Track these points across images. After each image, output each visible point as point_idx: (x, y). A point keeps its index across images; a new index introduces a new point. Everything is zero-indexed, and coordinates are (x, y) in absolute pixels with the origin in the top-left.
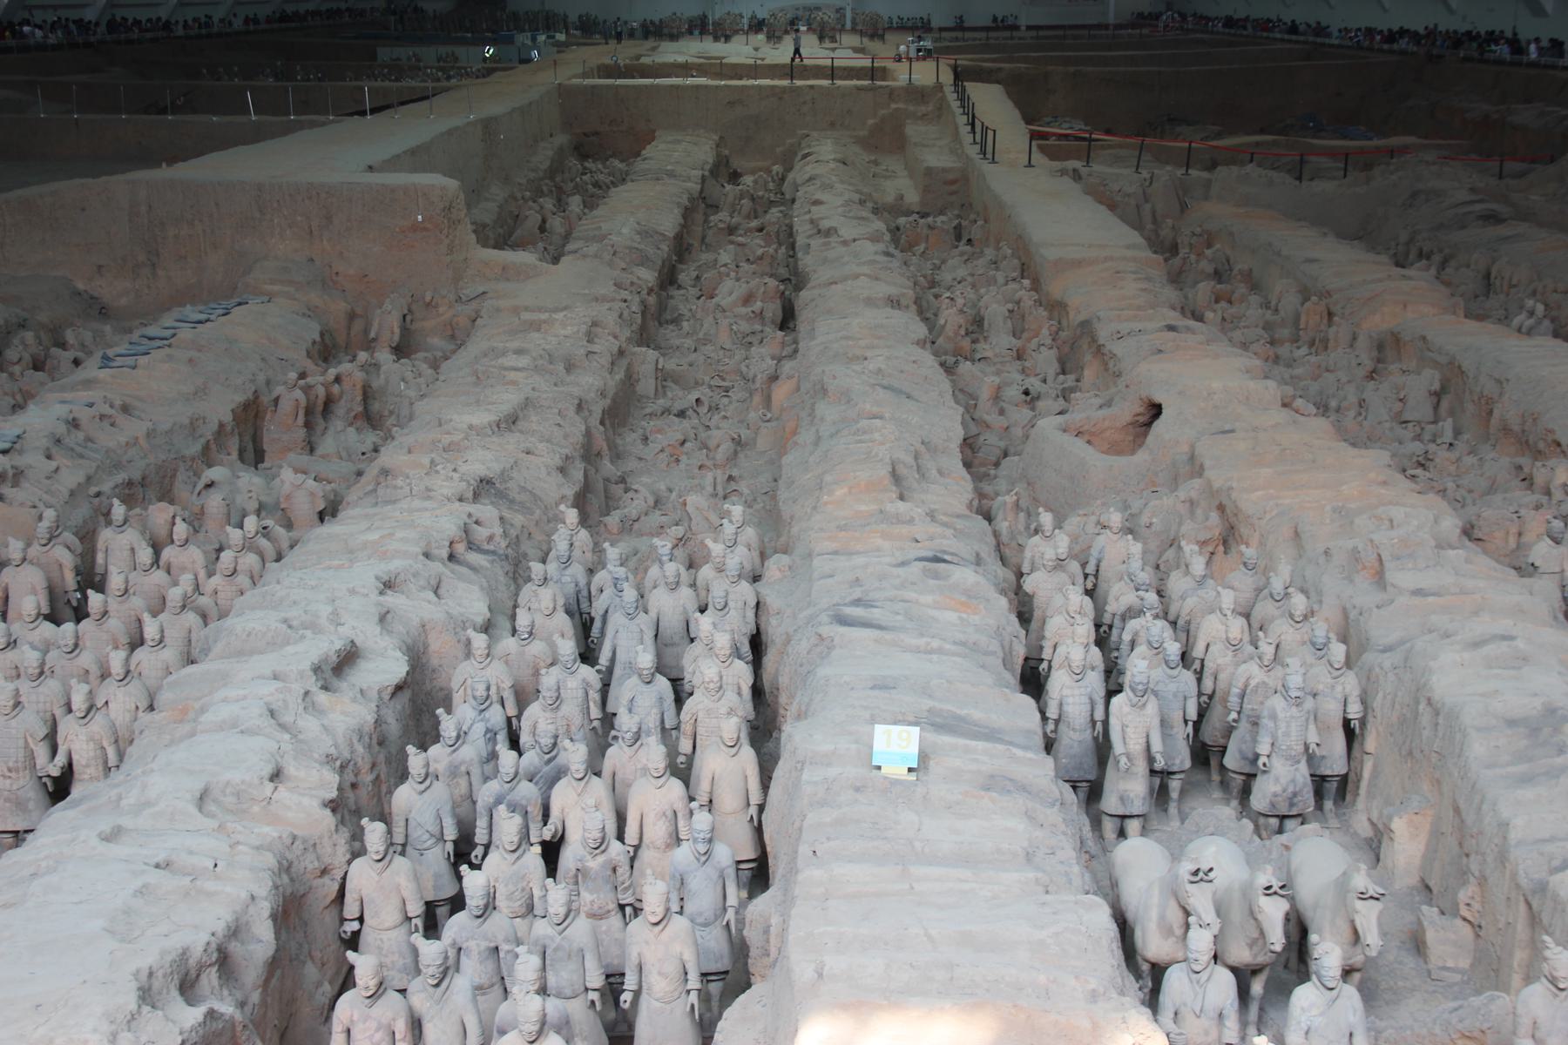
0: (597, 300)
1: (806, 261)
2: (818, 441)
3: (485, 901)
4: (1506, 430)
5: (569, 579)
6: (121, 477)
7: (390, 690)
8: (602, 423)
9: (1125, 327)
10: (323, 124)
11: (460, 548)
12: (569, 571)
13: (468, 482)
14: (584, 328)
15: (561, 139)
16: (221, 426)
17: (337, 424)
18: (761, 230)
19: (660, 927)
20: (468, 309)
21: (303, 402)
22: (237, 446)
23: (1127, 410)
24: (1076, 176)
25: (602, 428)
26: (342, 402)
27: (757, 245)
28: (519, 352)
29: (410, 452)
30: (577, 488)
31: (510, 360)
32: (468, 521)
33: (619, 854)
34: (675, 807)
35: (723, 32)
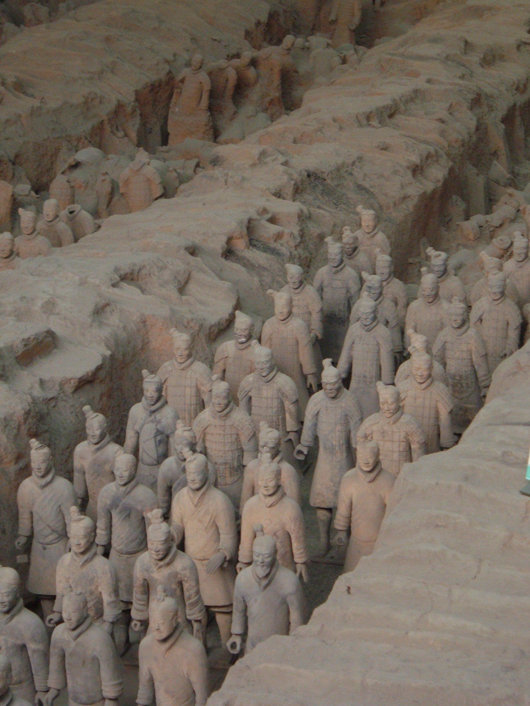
3: (10, 598)
5: (339, 284)
7: (73, 383)
8: (508, 120)
11: (240, 245)
12: (339, 276)
13: (290, 175)
16: (120, 106)
17: (248, 109)
19: (167, 645)
21: (207, 87)
22: (137, 126)
25: (503, 126)
26: (257, 88)
28: (435, 40)
30: (429, 186)
31: (425, 49)
32: (255, 216)
33: (185, 569)
34: (288, 528)
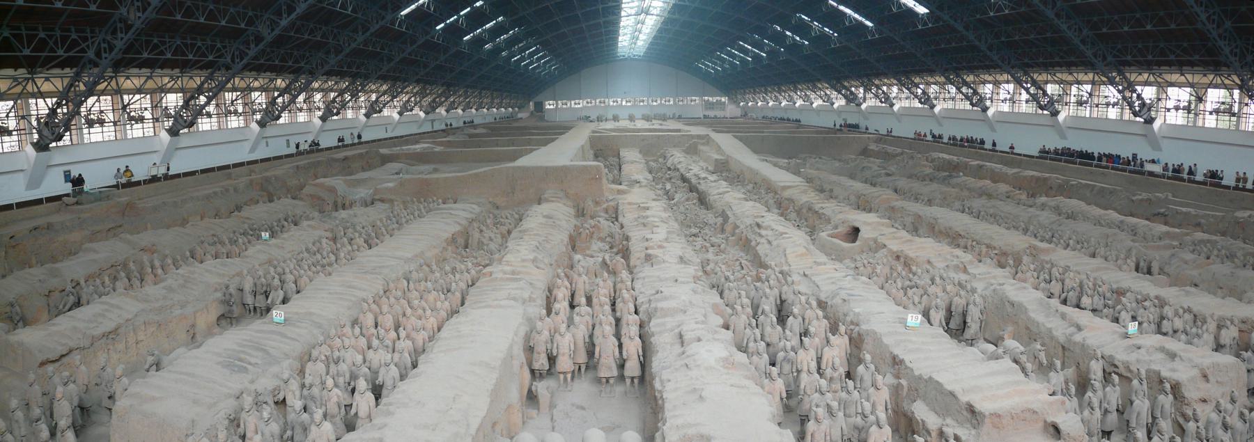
0: (654, 200)
1: (702, 187)
2: (769, 242)
4: (940, 232)
6: (555, 258)
9: (823, 205)
10: (535, 150)
14: (662, 209)
15: (592, 152)
17: (593, 241)
18: (670, 179)
20: (612, 204)
23: (842, 229)
24: (766, 160)
27: (679, 183)
28: (654, 217)
29: (647, 249)
35: (616, 118)
